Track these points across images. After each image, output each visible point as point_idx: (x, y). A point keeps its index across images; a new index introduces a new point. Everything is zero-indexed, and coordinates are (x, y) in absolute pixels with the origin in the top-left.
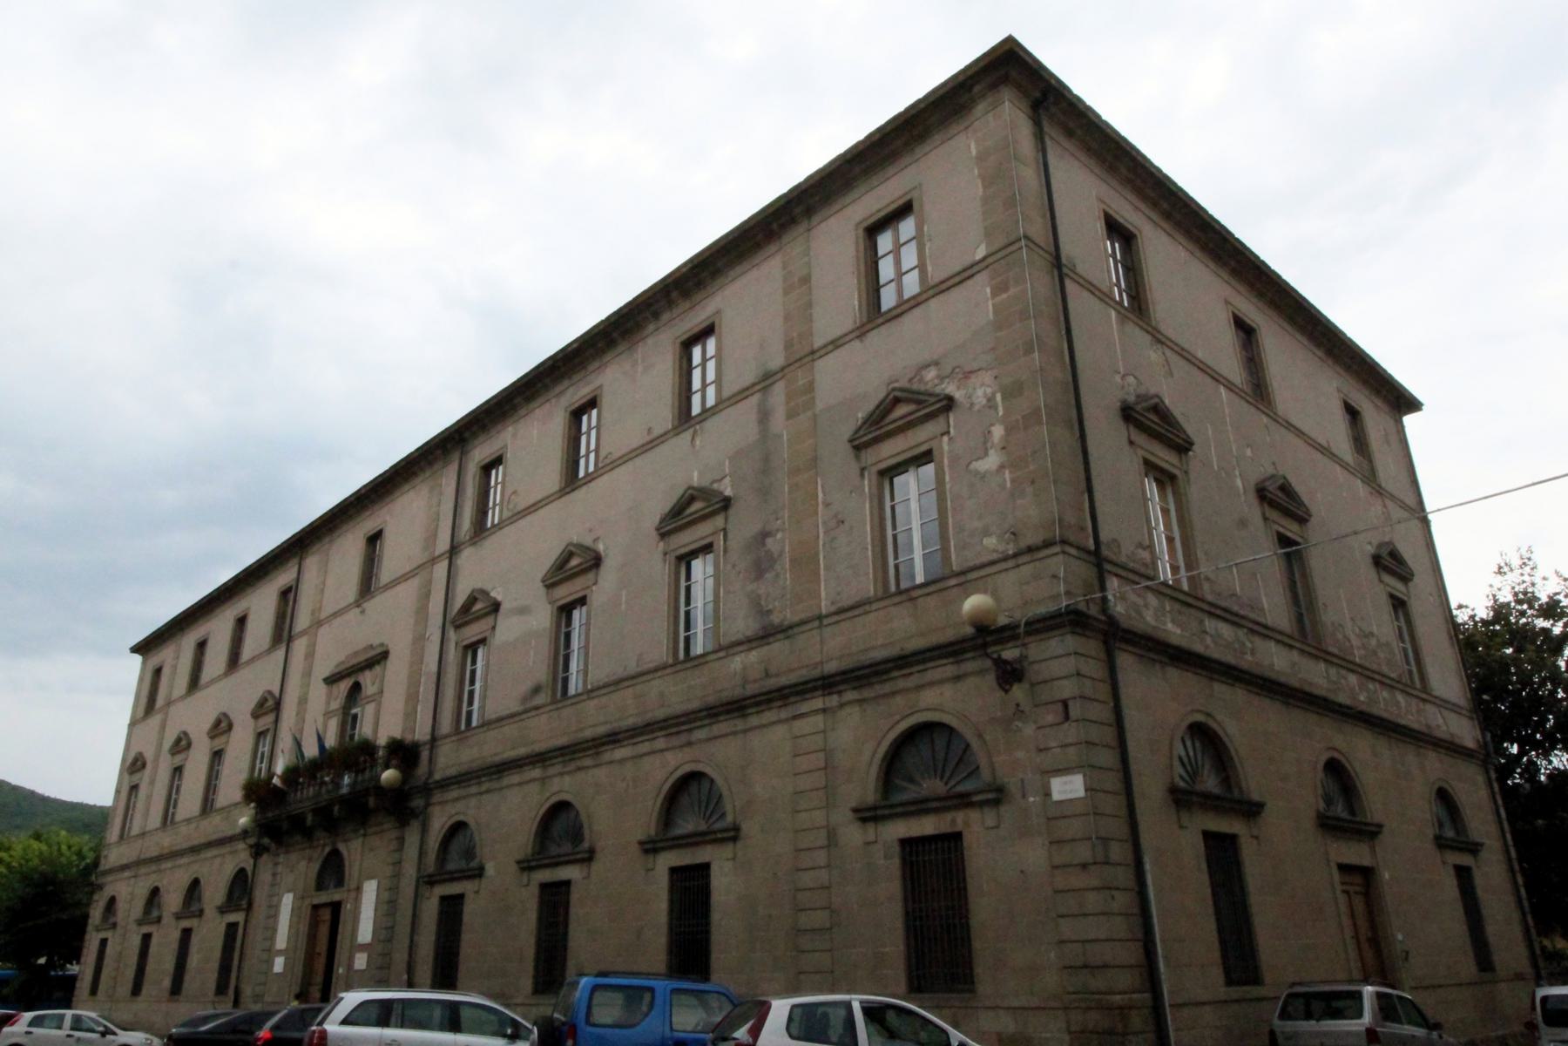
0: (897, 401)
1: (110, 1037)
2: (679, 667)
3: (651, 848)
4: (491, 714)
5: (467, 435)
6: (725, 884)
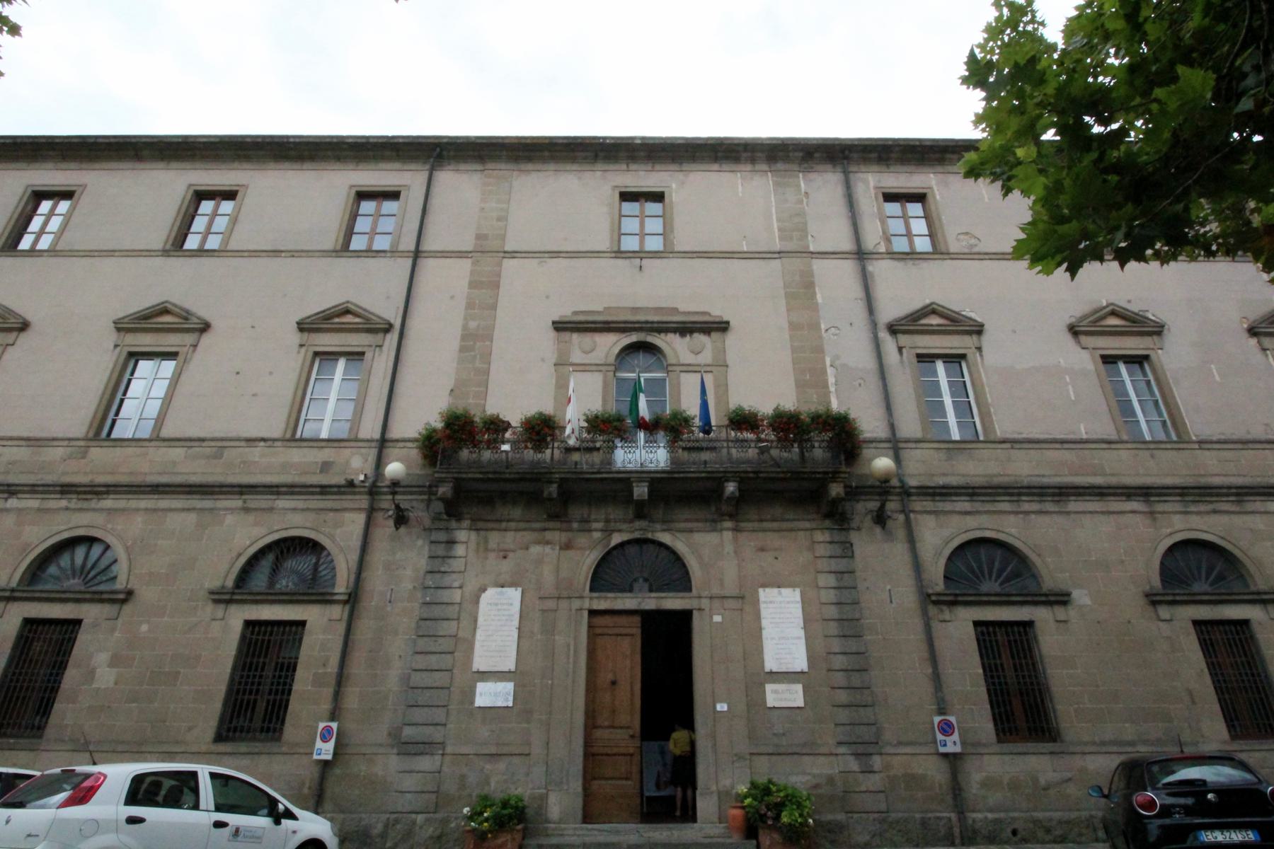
0: (934, 312)
1: (286, 823)
2: (293, 444)
3: (223, 598)
4: (306, 435)
5: (601, 154)
6: (1055, 638)
